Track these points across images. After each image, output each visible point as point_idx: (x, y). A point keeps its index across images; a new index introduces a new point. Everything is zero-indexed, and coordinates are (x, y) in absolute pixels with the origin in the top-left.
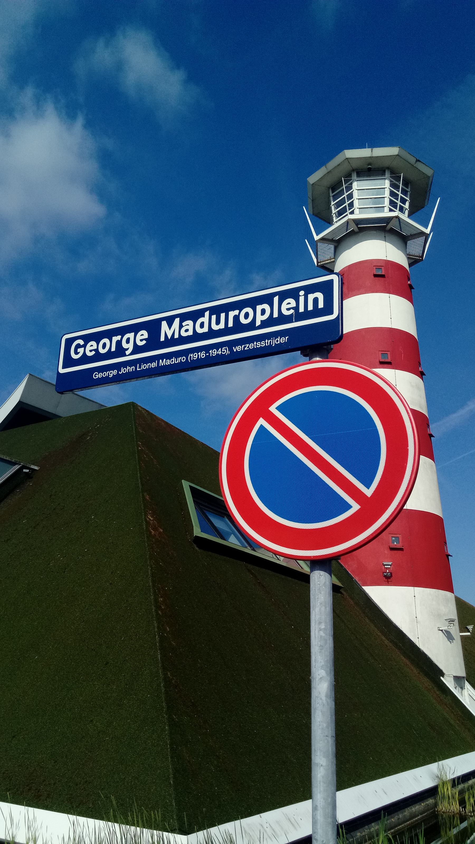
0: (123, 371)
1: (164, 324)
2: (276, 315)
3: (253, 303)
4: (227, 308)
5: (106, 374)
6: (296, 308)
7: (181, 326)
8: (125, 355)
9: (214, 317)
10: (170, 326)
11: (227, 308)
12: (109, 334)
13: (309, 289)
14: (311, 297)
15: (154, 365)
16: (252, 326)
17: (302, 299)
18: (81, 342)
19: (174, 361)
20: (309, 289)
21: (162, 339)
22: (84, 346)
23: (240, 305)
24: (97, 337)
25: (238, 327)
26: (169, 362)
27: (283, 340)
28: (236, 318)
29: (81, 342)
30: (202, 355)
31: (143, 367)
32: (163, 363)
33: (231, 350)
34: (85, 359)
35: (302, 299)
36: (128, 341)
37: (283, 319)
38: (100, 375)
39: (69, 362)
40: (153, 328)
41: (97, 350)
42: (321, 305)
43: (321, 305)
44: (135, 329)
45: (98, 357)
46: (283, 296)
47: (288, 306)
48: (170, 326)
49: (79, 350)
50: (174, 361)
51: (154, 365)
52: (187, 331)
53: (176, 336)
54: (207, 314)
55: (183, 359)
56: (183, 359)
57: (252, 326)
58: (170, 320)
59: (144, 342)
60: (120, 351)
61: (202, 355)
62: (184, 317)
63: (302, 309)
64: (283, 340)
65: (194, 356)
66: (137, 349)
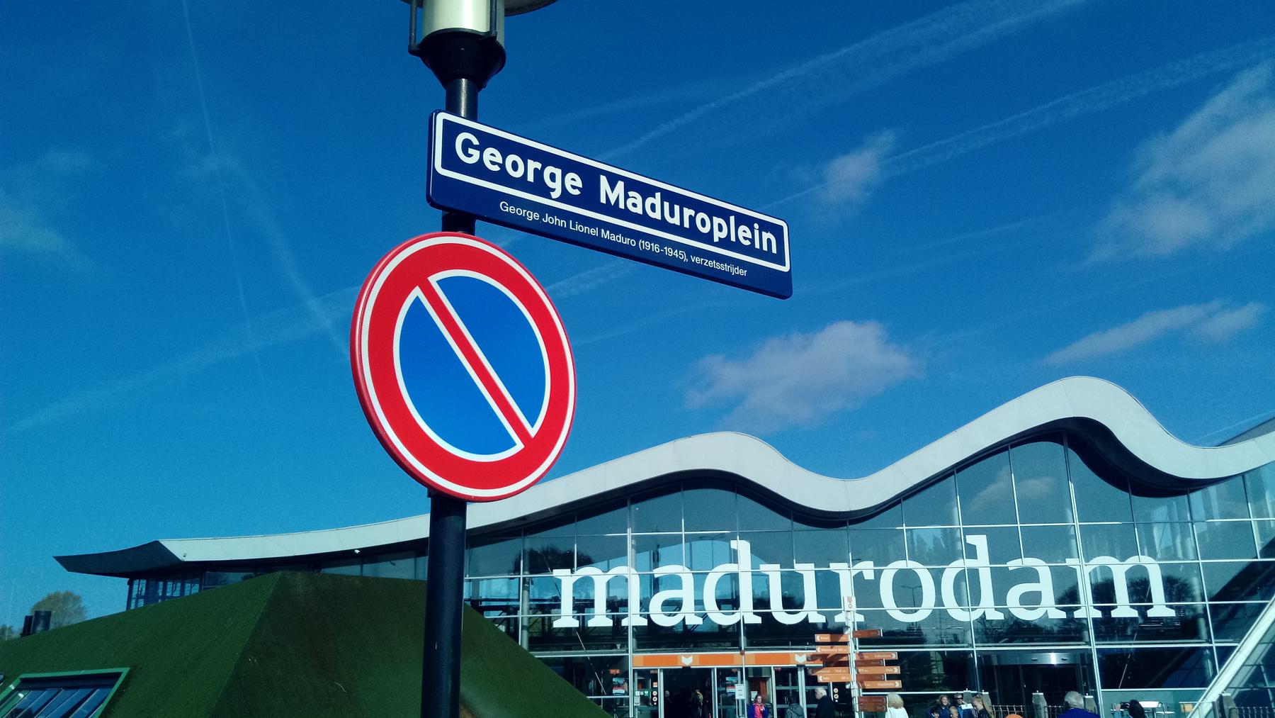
0: (547, 219)
1: (603, 180)
2: (733, 239)
3: (713, 211)
4: (685, 202)
5: (523, 212)
6: (752, 240)
7: (627, 197)
8: (549, 197)
9: (666, 204)
10: (613, 187)
11: (685, 202)
12: (527, 153)
13: (765, 227)
14: (766, 235)
15: (593, 232)
16: (708, 238)
17: (757, 232)
18: (476, 142)
19: (619, 238)
20: (765, 227)
21: (603, 200)
22: (481, 148)
23: (698, 206)
24: (506, 148)
25: (693, 232)
26: (614, 238)
27: (743, 272)
28: (692, 219)
29: (476, 142)
30: (656, 248)
31: (578, 227)
32: (606, 235)
33: (688, 257)
34: (478, 170)
35: (757, 232)
36: (553, 177)
37: (737, 246)
38: (511, 209)
39: (451, 160)
40: (591, 177)
41: (502, 166)
42: (774, 251)
43: (774, 251)
44: (567, 166)
45: (502, 177)
46: (741, 220)
47: (744, 232)
48: (613, 187)
49: (471, 151)
50: (619, 238)
51: (593, 232)
52: (634, 205)
53: (622, 206)
54: (658, 195)
55: (633, 242)
56: (633, 242)
57: (708, 238)
58: (613, 180)
59: (577, 192)
60: (540, 187)
61: (656, 248)
62: (631, 185)
63: (757, 246)
64: (743, 272)
65: (646, 245)
66: (565, 197)
